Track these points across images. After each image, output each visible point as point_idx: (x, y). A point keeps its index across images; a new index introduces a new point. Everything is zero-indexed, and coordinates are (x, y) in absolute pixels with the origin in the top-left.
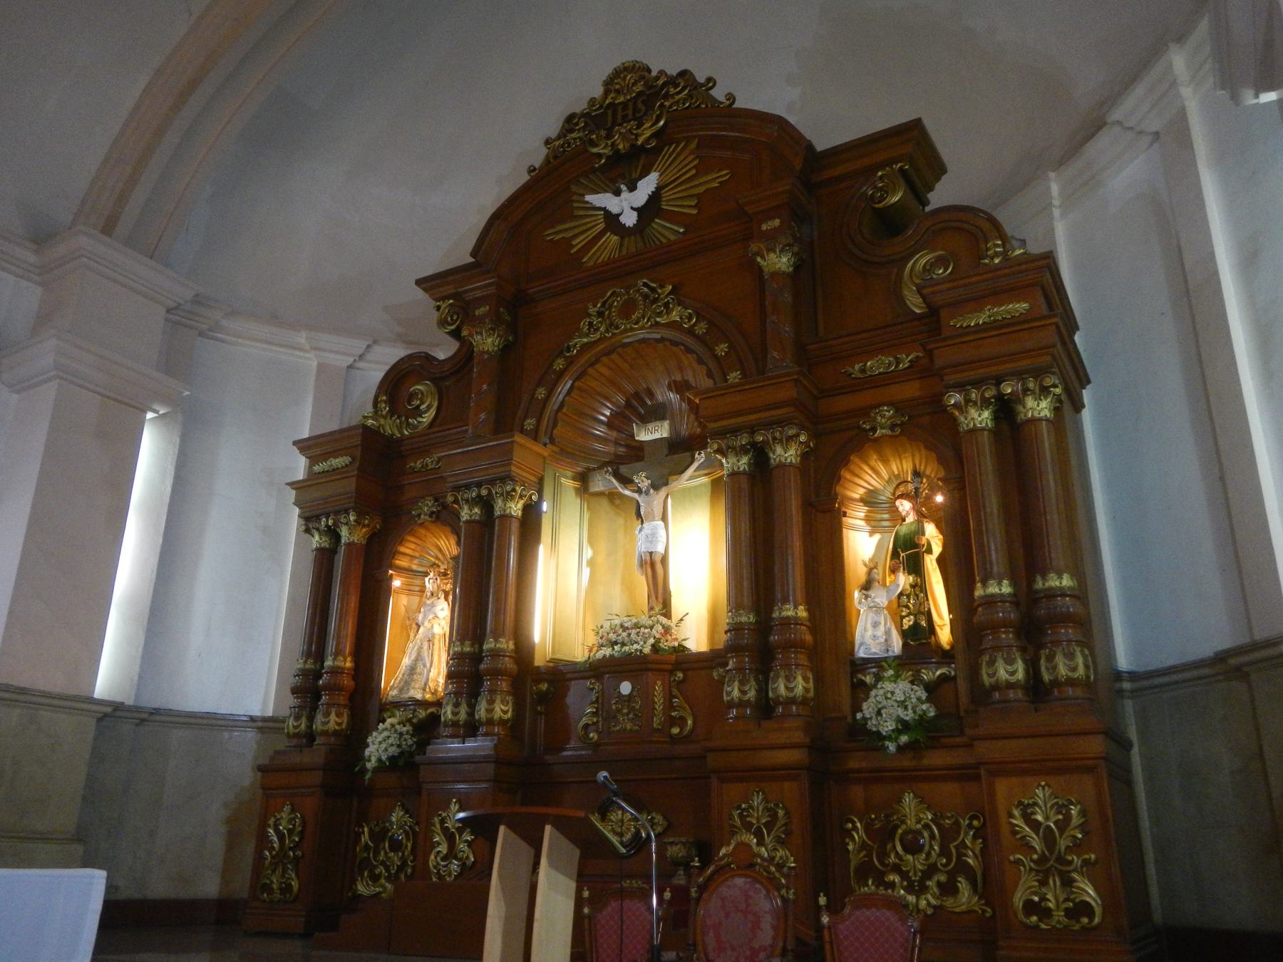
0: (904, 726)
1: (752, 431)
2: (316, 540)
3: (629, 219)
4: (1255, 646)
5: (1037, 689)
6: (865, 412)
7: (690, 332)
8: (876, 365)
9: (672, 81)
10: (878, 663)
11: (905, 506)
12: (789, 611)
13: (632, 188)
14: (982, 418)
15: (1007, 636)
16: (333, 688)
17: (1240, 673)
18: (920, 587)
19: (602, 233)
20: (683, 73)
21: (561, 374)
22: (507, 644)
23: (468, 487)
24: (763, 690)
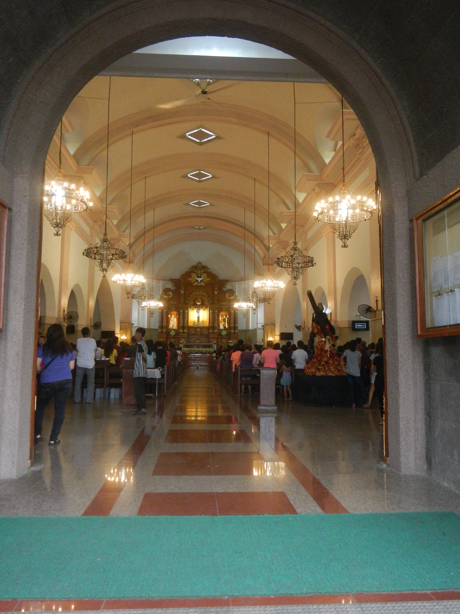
0: (225, 335)
1: (214, 309)
2: (160, 311)
3: (199, 281)
4: (247, 330)
5: (234, 333)
6: (223, 308)
7: (206, 296)
8: (224, 304)
9: (205, 267)
10: (222, 330)
11: (224, 316)
12: (216, 325)
13: (201, 277)
14: (233, 312)
15: (233, 329)
16: (165, 327)
17: (246, 331)
18: (225, 323)
19: (196, 281)
20: (207, 266)
21: (191, 297)
22: (187, 325)
23: (183, 308)
24: (213, 331)
